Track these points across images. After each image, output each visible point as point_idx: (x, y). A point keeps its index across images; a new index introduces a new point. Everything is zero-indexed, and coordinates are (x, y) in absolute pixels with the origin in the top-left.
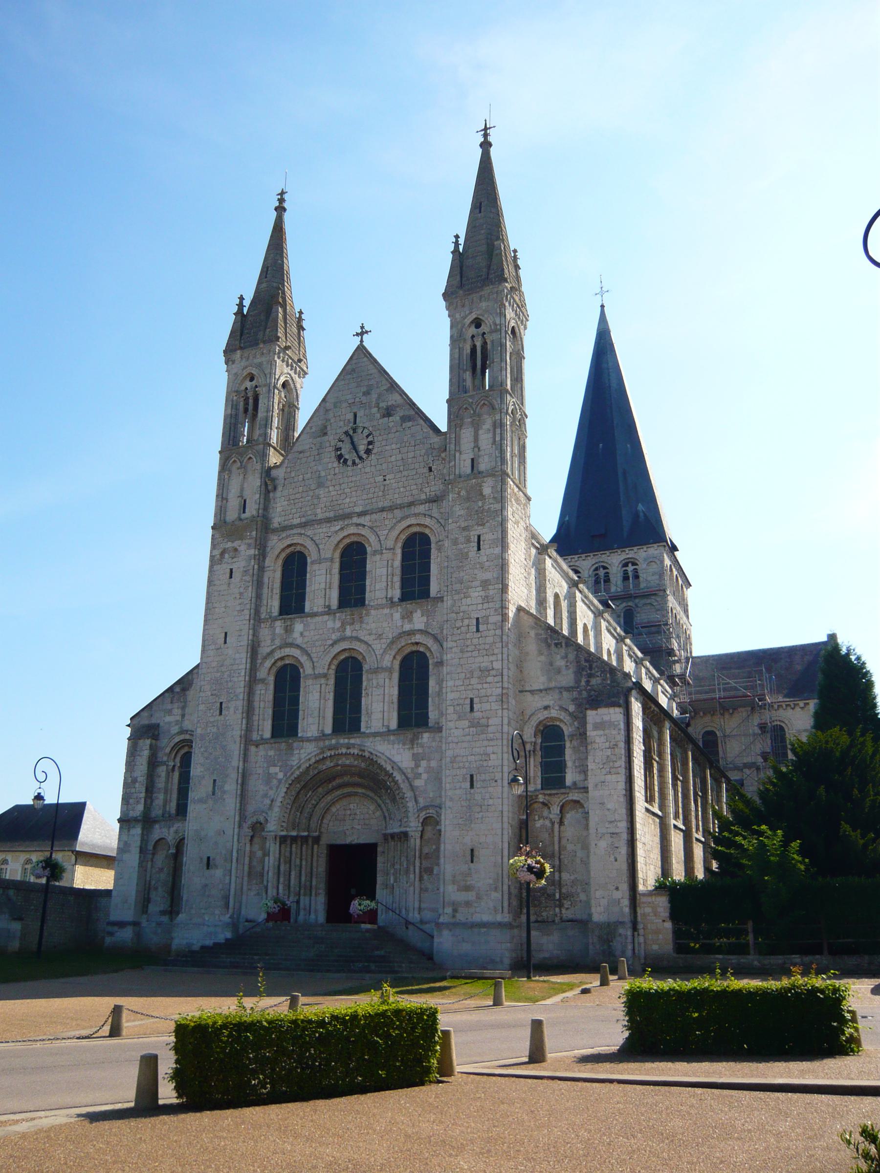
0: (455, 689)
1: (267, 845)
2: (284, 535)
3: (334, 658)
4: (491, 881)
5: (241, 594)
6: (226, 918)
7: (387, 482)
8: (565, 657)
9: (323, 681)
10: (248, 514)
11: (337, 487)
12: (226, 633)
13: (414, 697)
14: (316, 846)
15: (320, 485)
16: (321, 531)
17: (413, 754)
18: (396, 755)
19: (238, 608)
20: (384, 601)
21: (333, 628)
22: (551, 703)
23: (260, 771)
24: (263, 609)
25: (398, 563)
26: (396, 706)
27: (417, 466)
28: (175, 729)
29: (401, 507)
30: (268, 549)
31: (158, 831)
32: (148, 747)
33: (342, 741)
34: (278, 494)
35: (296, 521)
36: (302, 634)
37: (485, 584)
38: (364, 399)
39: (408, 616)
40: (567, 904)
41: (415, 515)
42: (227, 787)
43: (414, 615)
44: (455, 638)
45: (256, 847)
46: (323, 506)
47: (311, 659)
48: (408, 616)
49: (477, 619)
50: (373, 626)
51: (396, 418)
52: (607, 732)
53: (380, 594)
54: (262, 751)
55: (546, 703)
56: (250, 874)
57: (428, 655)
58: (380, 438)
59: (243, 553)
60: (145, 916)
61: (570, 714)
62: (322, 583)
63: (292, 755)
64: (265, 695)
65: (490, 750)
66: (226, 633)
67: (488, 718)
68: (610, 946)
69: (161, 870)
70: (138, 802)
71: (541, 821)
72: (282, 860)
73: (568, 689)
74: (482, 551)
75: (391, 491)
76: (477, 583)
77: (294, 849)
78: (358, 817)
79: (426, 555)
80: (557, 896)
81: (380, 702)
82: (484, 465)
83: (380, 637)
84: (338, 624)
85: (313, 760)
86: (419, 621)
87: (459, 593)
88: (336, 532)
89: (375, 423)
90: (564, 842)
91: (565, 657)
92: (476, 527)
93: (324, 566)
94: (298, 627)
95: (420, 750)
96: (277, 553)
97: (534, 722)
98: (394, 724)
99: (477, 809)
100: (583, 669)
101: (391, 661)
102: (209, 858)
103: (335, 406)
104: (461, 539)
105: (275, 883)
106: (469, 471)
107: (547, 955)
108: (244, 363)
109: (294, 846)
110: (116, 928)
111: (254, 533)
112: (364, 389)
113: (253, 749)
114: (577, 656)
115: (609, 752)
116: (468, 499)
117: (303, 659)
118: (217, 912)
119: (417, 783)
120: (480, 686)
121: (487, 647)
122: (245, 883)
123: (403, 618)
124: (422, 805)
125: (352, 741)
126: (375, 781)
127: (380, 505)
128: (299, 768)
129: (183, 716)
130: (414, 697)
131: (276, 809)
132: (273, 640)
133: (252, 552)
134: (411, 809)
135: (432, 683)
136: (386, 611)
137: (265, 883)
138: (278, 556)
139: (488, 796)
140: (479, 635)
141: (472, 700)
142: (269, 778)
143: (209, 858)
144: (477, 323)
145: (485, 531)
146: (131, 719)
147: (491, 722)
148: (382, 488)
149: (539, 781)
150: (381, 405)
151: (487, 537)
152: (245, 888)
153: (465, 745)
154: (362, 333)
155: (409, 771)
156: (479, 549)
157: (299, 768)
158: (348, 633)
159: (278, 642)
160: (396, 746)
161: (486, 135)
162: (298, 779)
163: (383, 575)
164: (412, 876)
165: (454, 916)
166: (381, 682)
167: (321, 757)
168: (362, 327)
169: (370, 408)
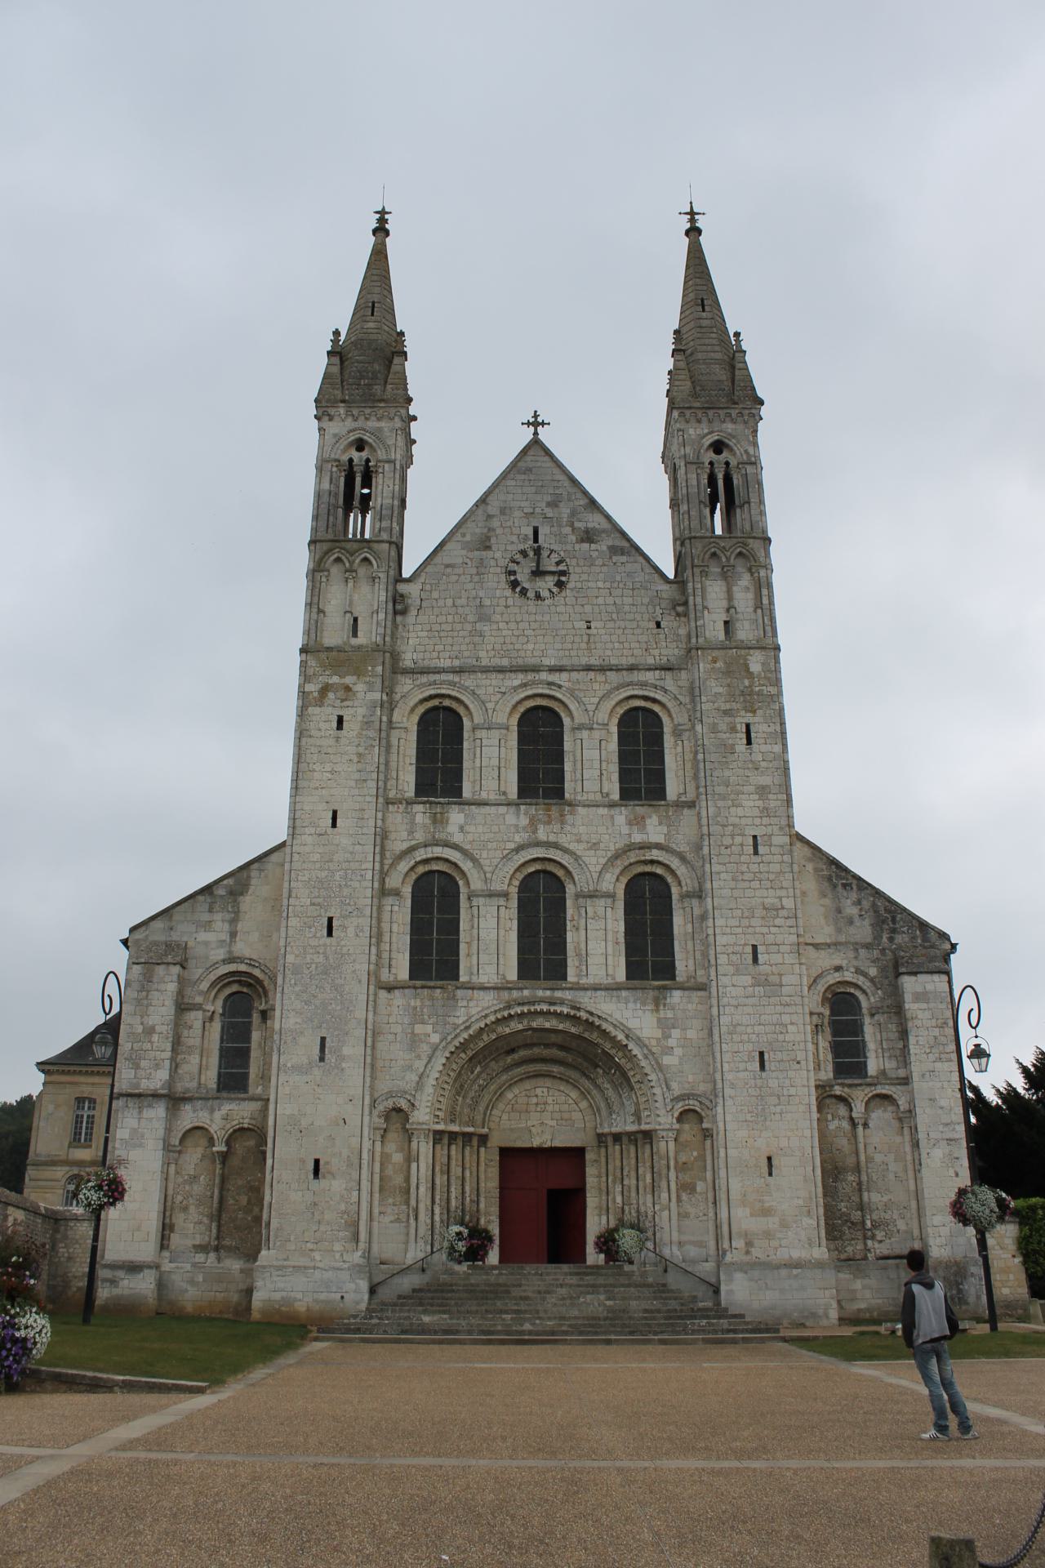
0: (728, 930)
1: (414, 1145)
2: (424, 679)
3: (518, 870)
4: (801, 1202)
5: (360, 755)
6: (357, 1257)
7: (593, 631)
8: (859, 902)
9: (502, 902)
10: (361, 639)
11: (513, 625)
12: (335, 813)
13: (649, 939)
14: (482, 1150)
15: (483, 618)
16: (488, 685)
17: (659, 1020)
18: (630, 1017)
19: (357, 776)
20: (598, 797)
21: (516, 826)
22: (844, 963)
23: (399, 1029)
24: (391, 783)
25: (613, 745)
26: (623, 947)
27: (638, 617)
28: (221, 954)
29: (617, 669)
30: (397, 697)
31: (191, 1114)
32: (175, 978)
33: (540, 993)
34: (411, 618)
35: (447, 663)
36: (462, 828)
37: (762, 791)
38: (549, 512)
40: (880, 1235)
41: (643, 685)
42: (346, 1051)
43: (648, 821)
45: (391, 1147)
46: (490, 647)
47: (481, 867)
48: (638, 822)
49: (755, 837)
50: (582, 829)
51: (603, 546)
52: (932, 1005)
53: (591, 786)
54: (398, 999)
55: (837, 962)
56: (381, 1190)
57: (669, 879)
58: (578, 570)
59: (360, 695)
60: (166, 1254)
61: (872, 980)
62: (491, 760)
63: (455, 1007)
64: (400, 916)
65: (786, 1019)
66: (335, 813)
67: (781, 975)
68: (960, 1291)
69: (194, 1178)
70: (157, 1067)
71: (836, 1122)
72: (437, 1169)
73: (867, 946)
74: (754, 746)
75: (599, 645)
76: (751, 789)
77: (453, 1152)
78: (550, 1108)
79: (656, 739)
80: (868, 1223)
81: (597, 941)
82: (745, 632)
83: (595, 846)
84: (524, 821)
85: (492, 1018)
86: (654, 830)
87: (724, 799)
88: (515, 689)
89: (569, 547)
90: (870, 1149)
91: (859, 902)
92: (743, 713)
93: (496, 734)
94: (456, 816)
95: (670, 1014)
96: (412, 704)
97: (821, 987)
98: (621, 975)
99: (773, 1100)
100: (883, 922)
101: (614, 883)
102: (317, 1162)
103: (503, 511)
104: (723, 727)
105: (429, 1203)
106: (722, 636)
107: (863, 1306)
108: (349, 423)
109: (453, 1147)
110: (121, 1274)
111: (379, 669)
112: (549, 498)
113: (383, 994)
114: (874, 905)
115: (936, 1032)
116: (728, 673)
117: (466, 866)
118: (338, 1247)
119: (667, 1060)
120: (765, 930)
121: (772, 877)
122: (376, 1203)
123: (630, 823)
124: (677, 1093)
125: (558, 994)
126: (587, 1055)
127: (584, 661)
128: (467, 1028)
130: (649, 939)
131: (429, 1090)
132: (411, 832)
133: (377, 696)
134: (659, 1098)
135: (680, 923)
136: (603, 811)
137: (413, 1203)
138: (412, 710)
139: (787, 1082)
140: (757, 859)
141: (754, 947)
142: (414, 1041)
143: (317, 1162)
144: (718, 447)
145: (756, 719)
146: (132, 930)
147: (785, 980)
148: (585, 638)
149: (830, 1067)
150: (577, 524)
151: (760, 730)
152: (376, 1211)
153: (749, 1010)
154: (536, 423)
155: (654, 1042)
156: (749, 742)
157: (467, 1028)
158: (542, 834)
159: (420, 836)
160: (631, 1005)
161: (692, 220)
162: (463, 1047)
163: (591, 760)
164: (665, 1195)
165: (748, 1252)
167: (506, 1014)
168: (536, 416)
169: (560, 526)
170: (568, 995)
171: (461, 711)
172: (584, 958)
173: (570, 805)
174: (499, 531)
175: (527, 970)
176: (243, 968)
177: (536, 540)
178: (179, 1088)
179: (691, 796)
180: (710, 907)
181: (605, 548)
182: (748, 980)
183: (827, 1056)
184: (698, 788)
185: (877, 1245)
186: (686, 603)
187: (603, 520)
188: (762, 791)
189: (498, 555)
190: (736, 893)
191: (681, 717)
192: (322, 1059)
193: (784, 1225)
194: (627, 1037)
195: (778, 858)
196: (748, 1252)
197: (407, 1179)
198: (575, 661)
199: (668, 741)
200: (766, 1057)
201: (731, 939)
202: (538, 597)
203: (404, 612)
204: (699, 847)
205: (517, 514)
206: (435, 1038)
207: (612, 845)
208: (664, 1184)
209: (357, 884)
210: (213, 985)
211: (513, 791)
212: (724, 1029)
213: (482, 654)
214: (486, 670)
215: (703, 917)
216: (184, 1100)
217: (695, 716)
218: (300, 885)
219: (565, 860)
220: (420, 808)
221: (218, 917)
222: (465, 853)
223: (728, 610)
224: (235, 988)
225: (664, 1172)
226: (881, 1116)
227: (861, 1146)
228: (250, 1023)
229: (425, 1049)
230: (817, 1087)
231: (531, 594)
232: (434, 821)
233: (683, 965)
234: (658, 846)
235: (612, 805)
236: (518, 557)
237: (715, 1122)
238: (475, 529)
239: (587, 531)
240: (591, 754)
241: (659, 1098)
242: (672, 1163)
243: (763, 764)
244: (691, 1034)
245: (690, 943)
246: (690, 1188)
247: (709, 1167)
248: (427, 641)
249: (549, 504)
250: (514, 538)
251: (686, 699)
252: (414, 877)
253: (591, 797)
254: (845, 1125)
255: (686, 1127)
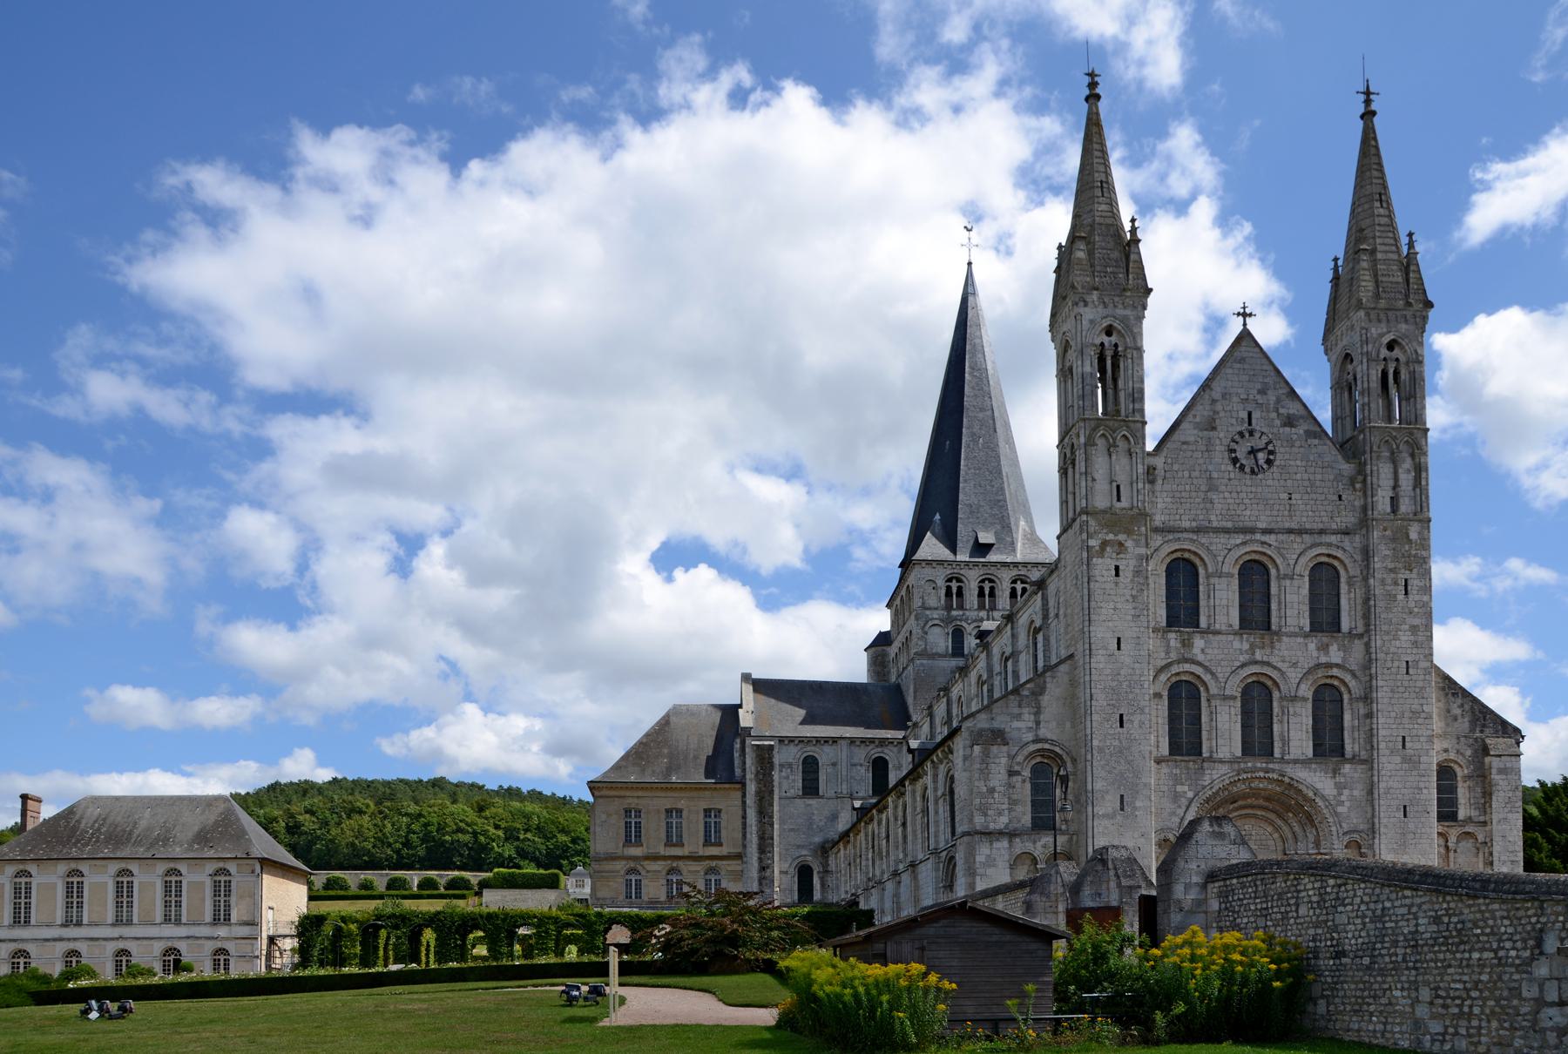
10: (1124, 503)
15: (1212, 488)
16: (1219, 542)
18: (1317, 781)
35: (1186, 524)
39: (1324, 648)
41: (1329, 545)
48: (1324, 648)
50: (1286, 653)
62: (1222, 600)
70: (1000, 814)
81: (1296, 731)
82: (1405, 507)
83: (1295, 665)
84: (1246, 646)
94: (1199, 643)
98: (1310, 754)
101: (1306, 691)
103: (1224, 396)
112: (1259, 386)
116: (1394, 540)
117: (1207, 678)
119: (1340, 809)
126: (1289, 805)
127: (1287, 525)
129: (1038, 723)
132: (1167, 653)
144: (1391, 346)
158: (1258, 657)
159: (1173, 656)
161: (1368, 102)
162: (1207, 801)
163: (1292, 601)
166: (1298, 710)
170: (1276, 766)
171: (1197, 562)
172: (1286, 742)
174: (1222, 414)
175: (1247, 749)
176: (1047, 746)
179: (1360, 629)
186: (1364, 481)
191: (1355, 570)
198: (1280, 525)
199: (1344, 587)
205: (1235, 399)
206: (1190, 795)
207: (1306, 664)
211: (1236, 623)
213: (1213, 518)
214: (1217, 530)
215: (1369, 715)
219: (1275, 674)
220: (1172, 636)
221: (1025, 710)
222: (1206, 668)
229: (1184, 802)
231: (1247, 469)
234: (1337, 665)
235: (1306, 636)
238: (1202, 412)
244: (1356, 793)
249: (1259, 392)
251: (1358, 557)
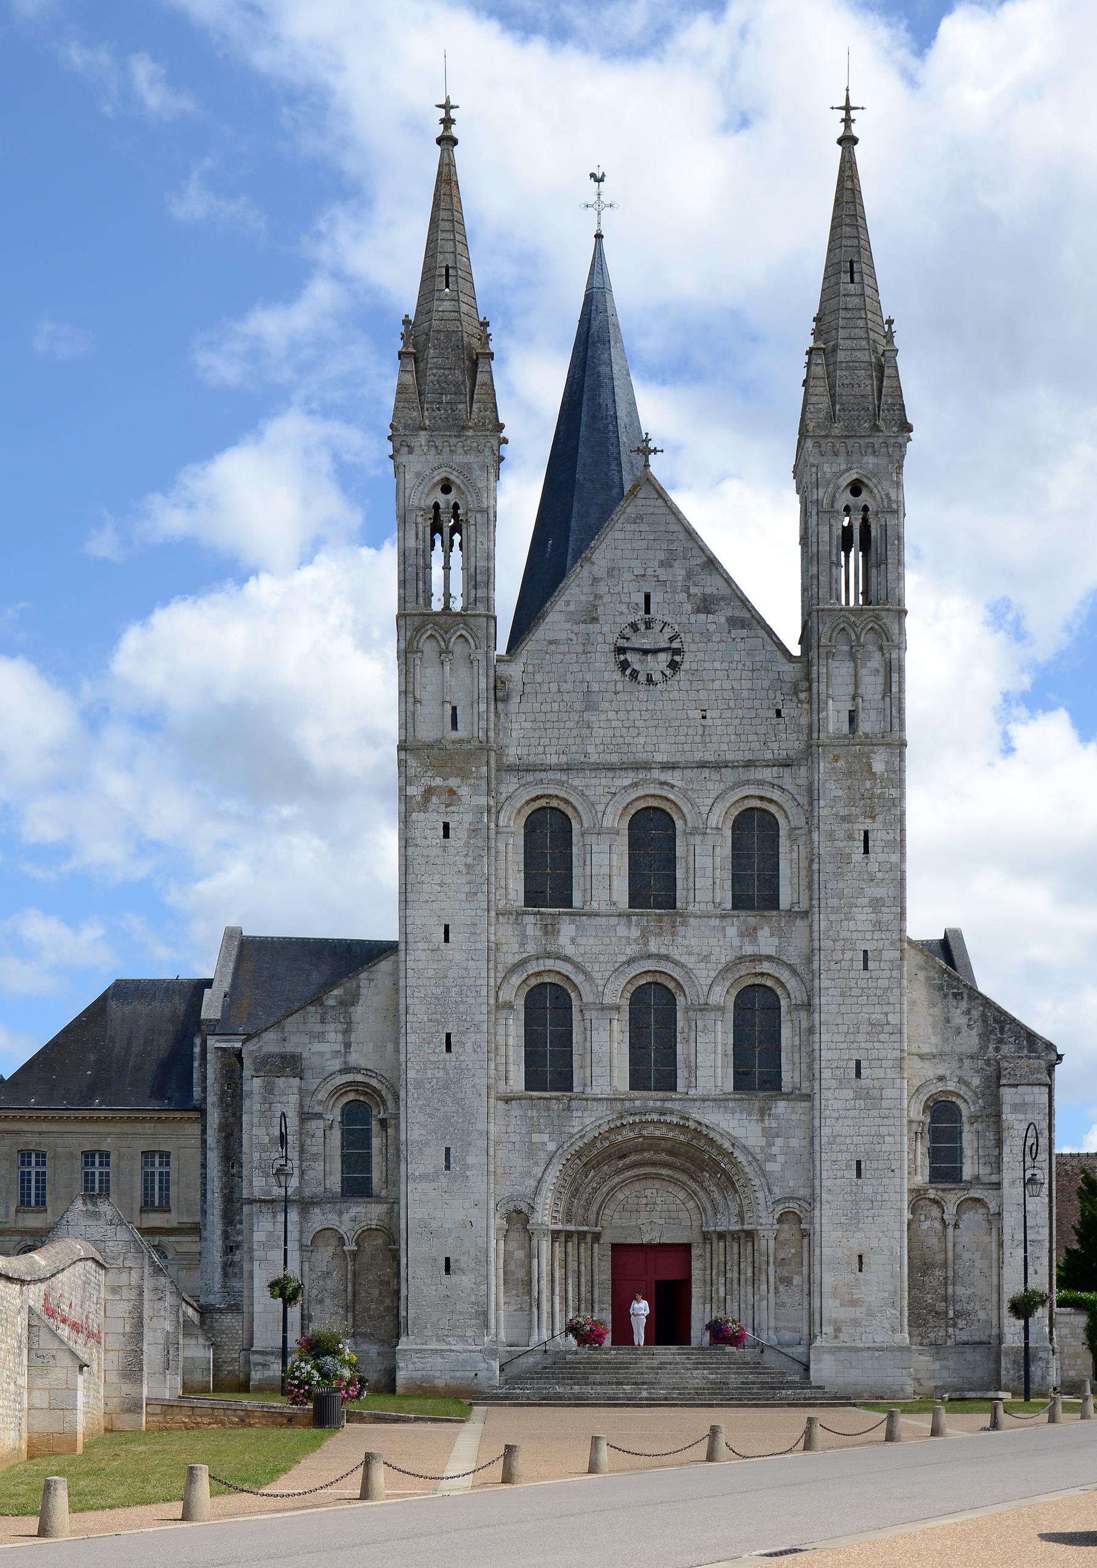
0: (833, 1046)
1: (534, 1243)
2: (530, 777)
10: (462, 733)
16: (597, 786)
18: (736, 1126)
27: (757, 703)
28: (336, 1064)
32: (296, 1090)
34: (513, 705)
35: (553, 760)
36: (573, 940)
37: (876, 904)
41: (760, 783)
43: (760, 933)
44: (831, 975)
45: (513, 1245)
46: (598, 741)
49: (865, 952)
54: (516, 1109)
58: (693, 647)
62: (604, 867)
65: (884, 1130)
69: (327, 1275)
74: (872, 855)
75: (714, 739)
76: (866, 900)
77: (570, 1249)
80: (951, 1314)
81: (708, 1054)
82: (867, 725)
83: (706, 959)
84: (635, 933)
92: (861, 819)
95: (774, 1124)
96: (518, 806)
98: (729, 1086)
99: (868, 1205)
103: (610, 572)
104: (840, 834)
109: (570, 1244)
116: (849, 774)
117: (578, 979)
119: (769, 1167)
120: (870, 1045)
123: (741, 935)
126: (698, 1160)
127: (698, 756)
128: (582, 1137)
129: (347, 1045)
132: (522, 945)
134: (762, 1201)
140: (865, 974)
141: (858, 1063)
145: (876, 825)
148: (700, 730)
153: (847, 1122)
155: (758, 1150)
156: (866, 851)
158: (653, 948)
159: (531, 949)
160: (737, 1116)
162: (578, 1154)
163: (705, 866)
173: (681, 916)
176: (359, 1078)
177: (647, 611)
178: (307, 1192)
179: (804, 906)
180: (817, 1022)
181: (723, 620)
182: (850, 1094)
183: (923, 1161)
184: (811, 899)
185: (957, 1332)
187: (722, 584)
188: (876, 904)
189: (606, 629)
190: (843, 1009)
192: (448, 1168)
193: (870, 1314)
194: (733, 1145)
195: (887, 974)
196: (836, 1337)
197: (529, 1273)
198: (688, 757)
200: (863, 1166)
201: (835, 1054)
202: (650, 680)
203: (506, 699)
204: (809, 961)
208: (764, 1277)
209: (472, 1001)
210: (332, 1094)
212: (824, 1140)
213: (591, 749)
214: (596, 768)
216: (313, 1204)
217: (811, 821)
218: (416, 1001)
221: (331, 1027)
222: (576, 965)
223: (854, 699)
224: (352, 1096)
225: (764, 1267)
226: (972, 1218)
227: (950, 1245)
228: (369, 1131)
230: (910, 1191)
232: (546, 933)
233: (788, 1077)
236: (628, 632)
237: (812, 1223)
239: (705, 598)
240: (703, 861)
241: (762, 1201)
242: (771, 1260)
243: (880, 875)
244: (794, 1143)
245: (797, 1056)
246: (787, 1281)
247: (805, 1263)
248: (531, 734)
250: (624, 608)
252: (527, 989)
253: (703, 907)
254: (937, 1225)
255: (786, 1226)
